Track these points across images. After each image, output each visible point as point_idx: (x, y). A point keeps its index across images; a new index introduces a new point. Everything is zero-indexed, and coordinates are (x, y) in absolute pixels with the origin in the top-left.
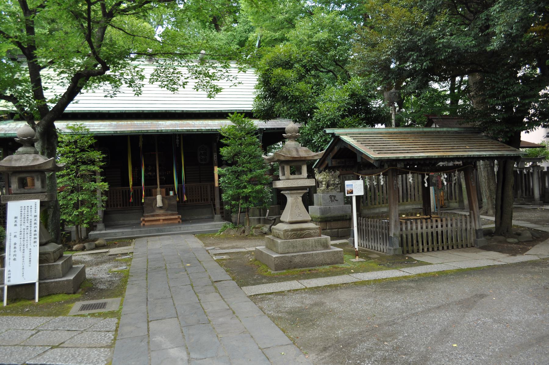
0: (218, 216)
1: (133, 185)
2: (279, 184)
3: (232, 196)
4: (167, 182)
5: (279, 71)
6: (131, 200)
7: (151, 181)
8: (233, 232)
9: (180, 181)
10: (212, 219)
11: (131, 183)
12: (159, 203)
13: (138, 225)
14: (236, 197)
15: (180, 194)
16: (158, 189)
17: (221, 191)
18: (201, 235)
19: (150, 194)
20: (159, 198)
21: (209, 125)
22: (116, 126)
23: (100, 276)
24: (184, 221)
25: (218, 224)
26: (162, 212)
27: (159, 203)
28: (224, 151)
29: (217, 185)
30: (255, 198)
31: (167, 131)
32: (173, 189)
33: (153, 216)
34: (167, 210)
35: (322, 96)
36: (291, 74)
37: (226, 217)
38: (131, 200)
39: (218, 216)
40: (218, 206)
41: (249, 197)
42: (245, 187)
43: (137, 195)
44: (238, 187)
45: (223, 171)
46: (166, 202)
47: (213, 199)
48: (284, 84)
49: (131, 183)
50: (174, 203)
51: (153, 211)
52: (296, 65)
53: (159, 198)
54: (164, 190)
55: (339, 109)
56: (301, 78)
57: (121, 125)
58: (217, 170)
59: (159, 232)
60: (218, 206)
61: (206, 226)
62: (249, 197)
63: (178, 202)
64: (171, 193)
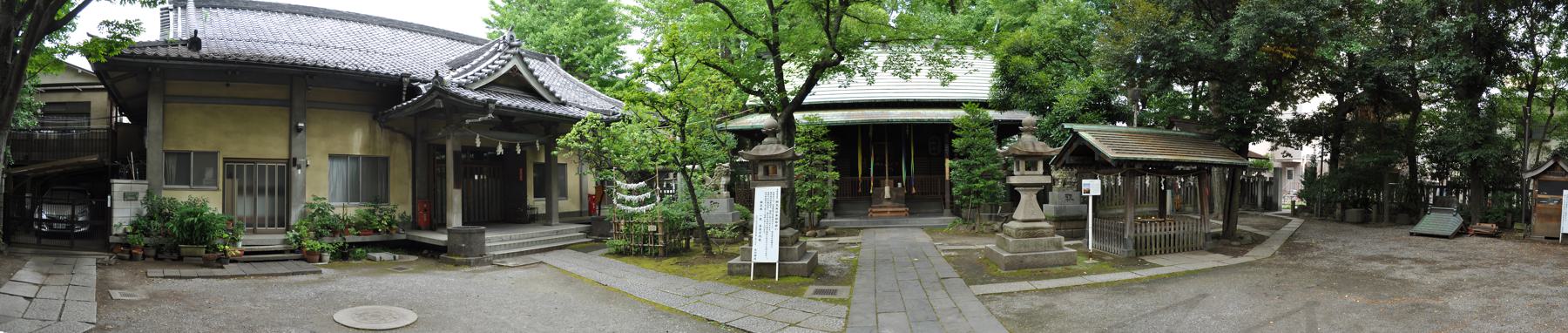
0: (947, 211)
2: (1013, 180)
4: (895, 173)
5: (1018, 58)
7: (879, 172)
8: (962, 229)
9: (908, 173)
10: (940, 213)
12: (887, 195)
14: (967, 192)
15: (908, 185)
17: (952, 185)
18: (930, 230)
19: (878, 184)
20: (887, 189)
23: (831, 263)
24: (912, 214)
25: (947, 219)
27: (887, 195)
28: (956, 143)
36: (1030, 63)
37: (956, 212)
43: (866, 185)
44: (970, 181)
45: (955, 163)
47: (943, 194)
53: (887, 189)
55: (1079, 103)
56: (1041, 67)
58: (948, 162)
59: (886, 224)
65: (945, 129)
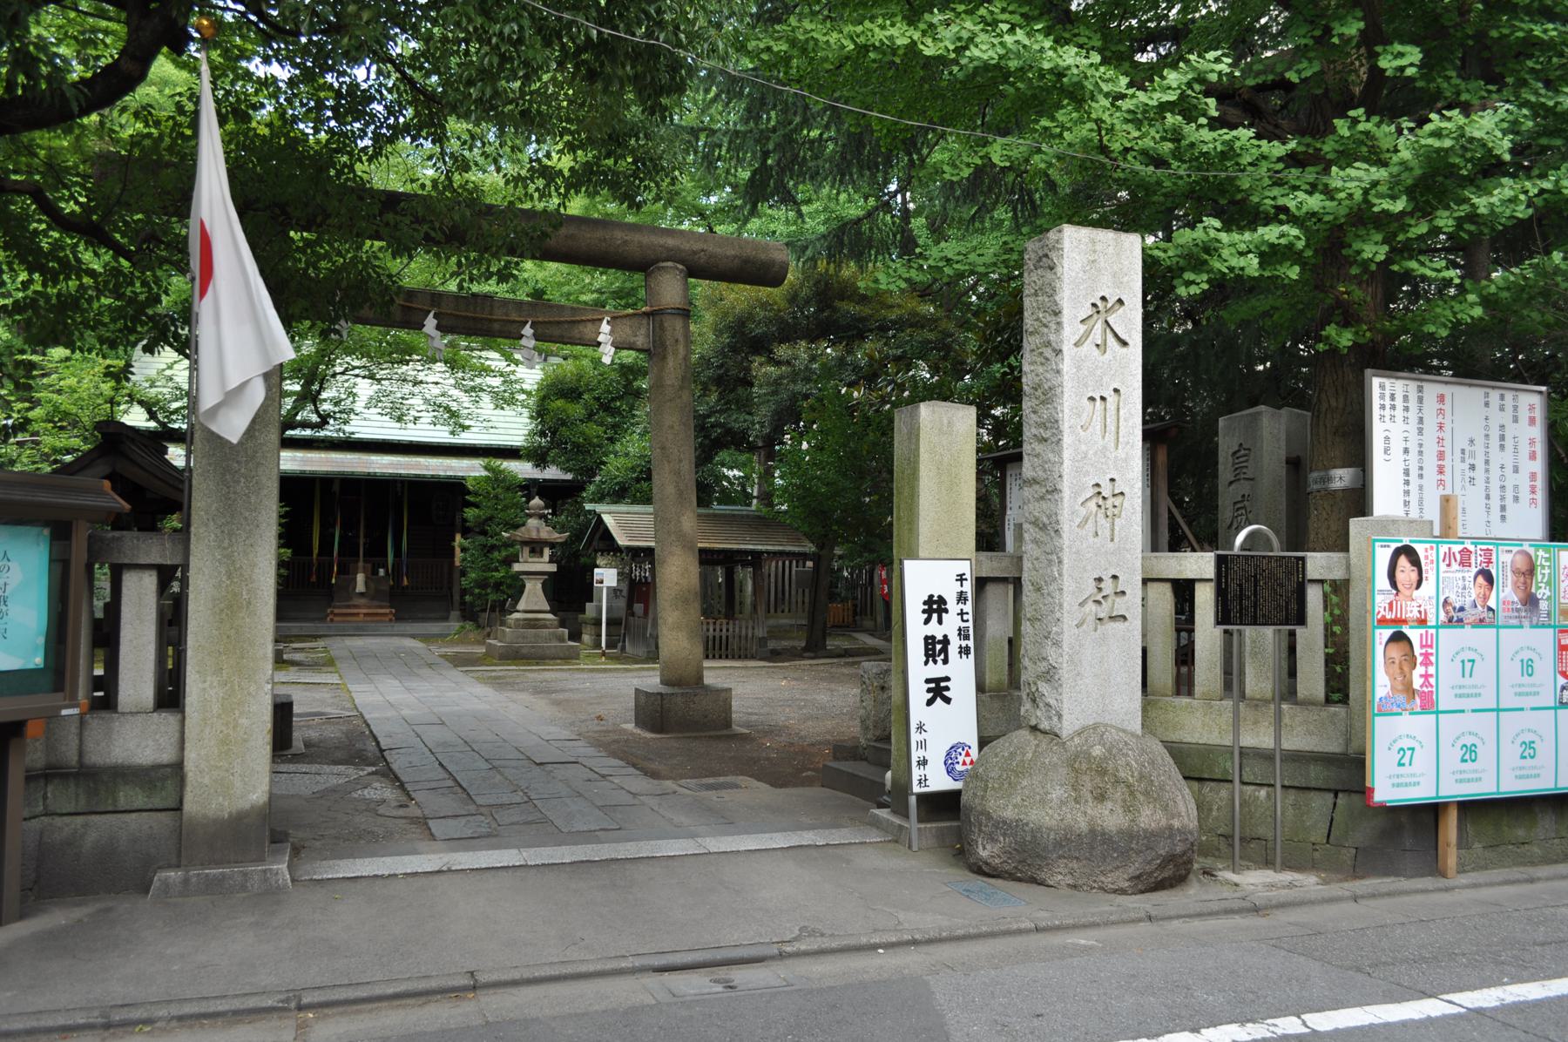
0: (455, 614)
1: (319, 554)
2: (517, 567)
3: (476, 581)
4: (376, 553)
5: (560, 403)
6: (314, 579)
7: (349, 550)
8: (472, 636)
9: (397, 553)
10: (446, 619)
11: (316, 551)
12: (360, 586)
13: (323, 620)
14: (482, 584)
15: (397, 573)
16: (361, 564)
17: (463, 573)
18: (426, 638)
19: (347, 571)
20: (360, 578)
21: (451, 468)
22: (302, 460)
24: (399, 618)
25: (454, 625)
26: (362, 601)
27: (360, 586)
28: (470, 513)
29: (457, 563)
30: (509, 586)
31: (383, 475)
32: (385, 566)
33: (349, 607)
34: (373, 599)
35: (618, 447)
36: (576, 410)
37: (469, 614)
38: (314, 579)
39: (455, 614)
40: (457, 597)
41: (501, 584)
42: (497, 570)
44: (487, 568)
45: (466, 543)
46: (372, 586)
47: (450, 588)
48: (564, 423)
49: (316, 551)
50: (385, 588)
51: (350, 598)
52: (586, 396)
53: (360, 578)
54: (369, 566)
55: (633, 469)
57: (311, 461)
58: (458, 537)
60: (457, 597)
61: (434, 628)
62: (501, 584)
63: (392, 588)
64: (382, 572)
65: (454, 489)
